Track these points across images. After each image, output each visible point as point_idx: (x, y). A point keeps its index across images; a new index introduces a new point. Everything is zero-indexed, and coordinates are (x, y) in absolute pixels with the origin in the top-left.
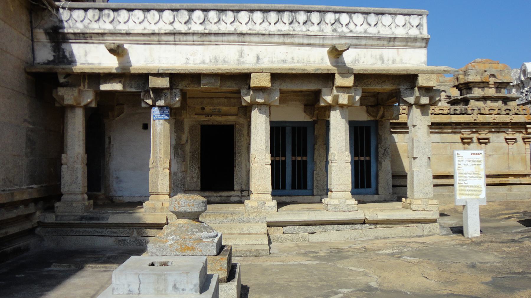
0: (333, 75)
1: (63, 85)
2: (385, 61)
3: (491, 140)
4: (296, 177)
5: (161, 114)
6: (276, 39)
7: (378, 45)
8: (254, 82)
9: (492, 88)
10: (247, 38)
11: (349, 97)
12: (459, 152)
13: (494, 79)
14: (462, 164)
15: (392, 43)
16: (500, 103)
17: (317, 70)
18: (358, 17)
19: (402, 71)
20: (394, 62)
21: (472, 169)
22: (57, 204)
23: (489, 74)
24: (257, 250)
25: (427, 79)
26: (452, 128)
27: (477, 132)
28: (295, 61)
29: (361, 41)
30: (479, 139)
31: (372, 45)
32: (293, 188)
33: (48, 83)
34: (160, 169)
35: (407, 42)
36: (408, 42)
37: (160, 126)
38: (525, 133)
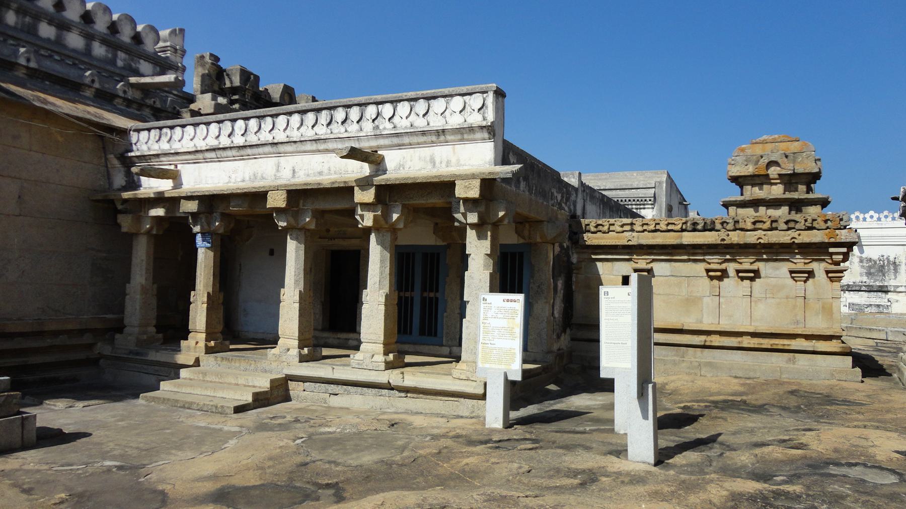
0: (353, 187)
1: (121, 212)
2: (437, 164)
3: (763, 274)
4: (333, 320)
5: (203, 241)
6: (308, 146)
7: (425, 143)
8: (460, 192)
9: (776, 184)
10: (281, 148)
11: (374, 216)
12: (486, 297)
13: (778, 168)
14: (489, 315)
15: (442, 138)
16: (785, 209)
17: (333, 183)
18: (403, 106)
19: (433, 178)
20: (448, 164)
21: (503, 323)
22: (118, 336)
23: (767, 161)
24: (222, 407)
25: (465, 187)
26: (689, 254)
27: (734, 260)
28: (332, 172)
29: (400, 140)
30: (738, 271)
31: (419, 144)
32: (422, 333)
33: (109, 210)
34: (199, 303)
35: (462, 134)
36: (465, 133)
37: (294, 253)
38: (830, 261)
